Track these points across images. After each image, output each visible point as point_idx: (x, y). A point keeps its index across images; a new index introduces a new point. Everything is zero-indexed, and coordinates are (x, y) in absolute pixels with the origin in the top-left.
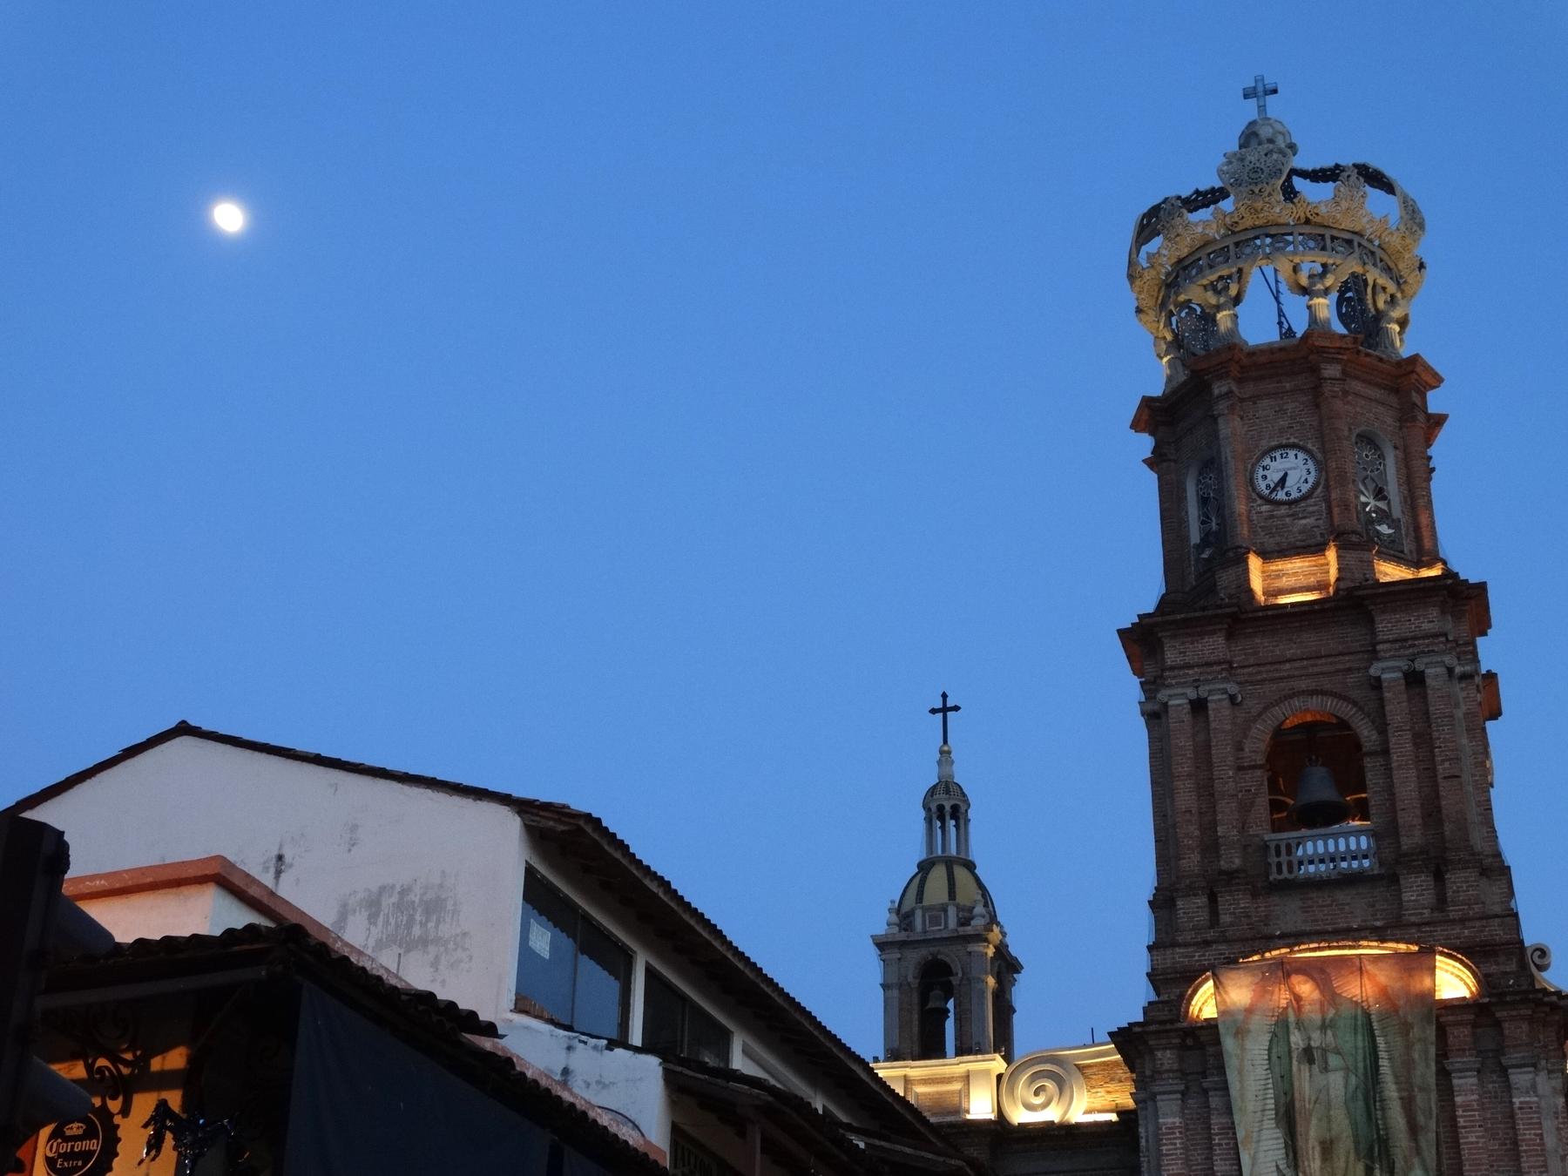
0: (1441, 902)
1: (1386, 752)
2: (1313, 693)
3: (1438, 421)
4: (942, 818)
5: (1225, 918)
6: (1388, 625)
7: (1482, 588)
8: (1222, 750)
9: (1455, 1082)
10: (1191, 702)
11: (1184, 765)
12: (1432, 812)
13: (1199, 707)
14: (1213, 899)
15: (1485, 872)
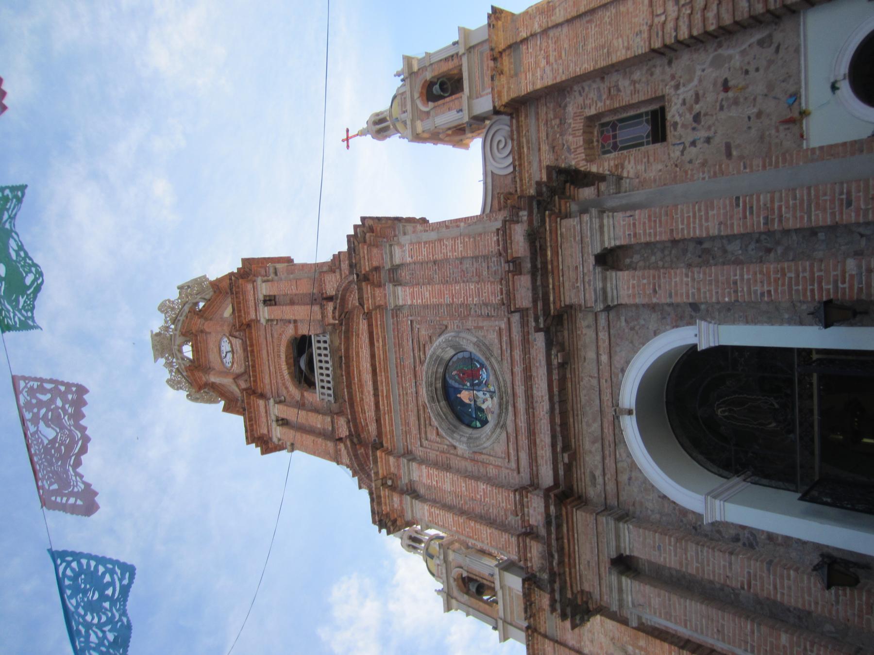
1: (295, 321)
2: (279, 356)
7: (244, 261)
9: (401, 303)
13: (283, 422)
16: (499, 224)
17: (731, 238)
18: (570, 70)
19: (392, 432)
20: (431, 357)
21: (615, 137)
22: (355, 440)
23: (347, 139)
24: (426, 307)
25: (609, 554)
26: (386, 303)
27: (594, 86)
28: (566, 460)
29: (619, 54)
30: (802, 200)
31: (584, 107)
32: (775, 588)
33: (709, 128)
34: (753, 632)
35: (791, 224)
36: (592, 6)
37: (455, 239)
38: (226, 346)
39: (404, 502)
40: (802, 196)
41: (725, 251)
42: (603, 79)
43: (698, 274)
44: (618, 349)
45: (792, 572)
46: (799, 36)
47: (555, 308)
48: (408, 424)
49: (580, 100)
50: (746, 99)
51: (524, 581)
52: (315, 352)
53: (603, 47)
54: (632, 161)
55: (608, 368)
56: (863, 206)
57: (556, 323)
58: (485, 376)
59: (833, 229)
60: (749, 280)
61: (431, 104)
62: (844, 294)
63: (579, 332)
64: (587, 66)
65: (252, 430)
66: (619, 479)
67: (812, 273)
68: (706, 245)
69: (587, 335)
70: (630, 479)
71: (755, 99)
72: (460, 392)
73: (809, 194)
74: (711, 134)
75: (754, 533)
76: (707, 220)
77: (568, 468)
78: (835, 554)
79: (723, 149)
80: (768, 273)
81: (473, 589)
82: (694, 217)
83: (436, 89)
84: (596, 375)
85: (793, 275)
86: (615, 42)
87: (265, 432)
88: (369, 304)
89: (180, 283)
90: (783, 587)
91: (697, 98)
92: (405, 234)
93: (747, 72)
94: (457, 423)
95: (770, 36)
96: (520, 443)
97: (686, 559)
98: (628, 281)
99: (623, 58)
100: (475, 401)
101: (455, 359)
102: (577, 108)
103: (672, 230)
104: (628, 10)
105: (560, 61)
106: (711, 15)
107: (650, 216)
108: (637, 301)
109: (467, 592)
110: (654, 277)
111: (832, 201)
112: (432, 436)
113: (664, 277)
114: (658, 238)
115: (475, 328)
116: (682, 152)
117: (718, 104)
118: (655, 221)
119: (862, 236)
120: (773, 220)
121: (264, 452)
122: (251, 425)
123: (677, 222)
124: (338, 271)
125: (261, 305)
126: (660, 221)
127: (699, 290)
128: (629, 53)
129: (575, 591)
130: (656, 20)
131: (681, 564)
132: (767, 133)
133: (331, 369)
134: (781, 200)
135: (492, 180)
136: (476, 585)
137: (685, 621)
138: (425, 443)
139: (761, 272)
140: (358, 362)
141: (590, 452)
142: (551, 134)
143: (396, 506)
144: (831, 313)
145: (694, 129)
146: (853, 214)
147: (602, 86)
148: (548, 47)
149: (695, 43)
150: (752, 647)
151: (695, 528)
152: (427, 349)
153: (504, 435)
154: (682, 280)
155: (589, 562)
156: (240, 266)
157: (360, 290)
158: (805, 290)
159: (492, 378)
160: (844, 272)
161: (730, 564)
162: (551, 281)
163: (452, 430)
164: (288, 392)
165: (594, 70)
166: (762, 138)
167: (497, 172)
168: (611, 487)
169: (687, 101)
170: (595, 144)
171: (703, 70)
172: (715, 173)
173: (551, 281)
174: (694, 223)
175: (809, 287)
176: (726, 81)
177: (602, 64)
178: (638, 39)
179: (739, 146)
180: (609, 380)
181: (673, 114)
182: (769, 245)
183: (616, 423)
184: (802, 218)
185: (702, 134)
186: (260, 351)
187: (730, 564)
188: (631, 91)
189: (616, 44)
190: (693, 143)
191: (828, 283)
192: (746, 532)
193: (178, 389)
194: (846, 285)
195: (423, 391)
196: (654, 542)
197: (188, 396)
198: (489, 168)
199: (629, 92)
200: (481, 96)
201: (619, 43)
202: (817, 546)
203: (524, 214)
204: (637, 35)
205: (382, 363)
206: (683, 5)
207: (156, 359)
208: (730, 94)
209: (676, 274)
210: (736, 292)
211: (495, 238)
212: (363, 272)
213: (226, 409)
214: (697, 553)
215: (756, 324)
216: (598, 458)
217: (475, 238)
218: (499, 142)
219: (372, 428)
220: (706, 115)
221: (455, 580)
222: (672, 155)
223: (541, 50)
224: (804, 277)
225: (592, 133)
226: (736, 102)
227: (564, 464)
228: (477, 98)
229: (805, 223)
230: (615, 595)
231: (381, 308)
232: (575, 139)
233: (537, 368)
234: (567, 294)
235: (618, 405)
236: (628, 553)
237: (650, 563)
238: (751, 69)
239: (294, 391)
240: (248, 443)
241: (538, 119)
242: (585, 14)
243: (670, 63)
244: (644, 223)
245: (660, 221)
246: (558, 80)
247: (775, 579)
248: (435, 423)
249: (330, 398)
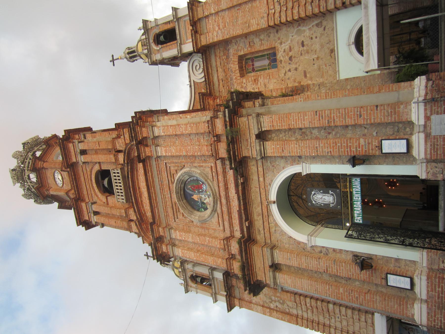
1: (99, 163)
2: (91, 180)
9: (160, 155)
10: (94, 215)
13: (96, 213)
16: (208, 118)
17: (313, 128)
18: (231, 33)
19: (159, 216)
20: (177, 180)
21: (253, 65)
22: (140, 221)
23: (113, 61)
24: (173, 157)
25: (268, 263)
26: (152, 155)
27: (242, 40)
28: (247, 225)
29: (254, 27)
30: (342, 114)
31: (238, 50)
32: (337, 270)
33: (296, 63)
34: (329, 289)
35: (338, 124)
36: (240, 2)
37: (186, 125)
38: (58, 177)
39: (169, 248)
40: (342, 112)
41: (312, 133)
42: (246, 37)
43: (302, 144)
44: (267, 175)
45: (343, 264)
46: (333, 23)
47: (238, 158)
48: (167, 212)
49: (236, 47)
50: (312, 51)
51: (223, 274)
52: (113, 178)
53: (246, 23)
54: (262, 78)
55: (263, 183)
56: (366, 118)
57: (240, 165)
58: (204, 188)
59: (355, 126)
60: (322, 146)
61: (160, 46)
62: (360, 153)
63: (249, 168)
64: (239, 32)
65: (80, 219)
66: (271, 231)
67: (347, 144)
68: (303, 131)
69: (253, 169)
70: (275, 231)
71: (316, 51)
72: (193, 196)
73: (345, 111)
74: (297, 66)
75: (327, 249)
76: (304, 120)
77: (248, 228)
78: (359, 254)
79: (303, 73)
80: (330, 144)
81: (199, 280)
82: (299, 119)
83: (162, 38)
84: (258, 187)
85: (340, 145)
86: (251, 20)
87: (87, 218)
88: (143, 156)
89: (23, 142)
90: (340, 270)
91: (290, 50)
92: (158, 121)
93: (312, 38)
94: (191, 209)
95: (321, 22)
96: (224, 218)
97: (301, 262)
98: (271, 146)
99: (256, 29)
100: (201, 200)
101: (189, 180)
102: (235, 52)
103: (289, 124)
104: (257, 5)
105: (226, 29)
106: (295, 11)
107: (279, 118)
108: (275, 155)
109: (196, 282)
110: (282, 145)
111: (354, 115)
112: (180, 217)
113: (287, 145)
114: (283, 128)
115: (199, 166)
116: (285, 75)
117: (300, 52)
118: (282, 120)
119: (365, 128)
120: (331, 121)
121: (86, 229)
122: (79, 216)
123: (291, 121)
124: (122, 137)
125: (79, 155)
126: (284, 120)
127: (302, 150)
128: (258, 27)
129: (254, 281)
130: (270, 11)
131: (299, 264)
132: (322, 67)
133: (123, 186)
134: (334, 113)
135: (194, 85)
136: (200, 278)
137: (302, 287)
138: (177, 220)
139: (327, 143)
140: (138, 183)
141: (257, 220)
142: (222, 63)
143: (164, 251)
144: (355, 161)
145: (289, 64)
146: (362, 121)
147: (246, 41)
148: (218, 20)
149: (289, 23)
150: (329, 294)
151: (304, 249)
152: (175, 176)
153: (216, 215)
154: (294, 146)
155: (260, 268)
156: (64, 134)
157: (138, 149)
158: (345, 151)
159: (208, 188)
160: (359, 144)
161: (319, 263)
162: (236, 146)
163: (191, 213)
164: (98, 198)
165: (242, 34)
166: (319, 69)
167: (196, 80)
168: (267, 235)
169: (286, 50)
170: (244, 68)
171: (293, 36)
172: (306, 98)
173: (236, 146)
174: (299, 122)
175: (346, 150)
176: (303, 42)
177: (246, 31)
178: (262, 21)
179: (310, 72)
180: (264, 189)
181: (280, 55)
182: (329, 131)
183: (268, 206)
184: (342, 121)
185: (293, 66)
186: (79, 178)
187: (319, 263)
188: (260, 45)
189: (252, 22)
190: (290, 70)
191: (353, 148)
192: (325, 249)
193: (29, 199)
194: (360, 149)
195: (174, 196)
196: (288, 256)
197: (35, 201)
198: (193, 78)
199: (259, 45)
200: (186, 43)
201: (253, 22)
202: (352, 252)
203: (220, 114)
204: (262, 18)
205: (152, 183)
206: (282, 6)
207: (14, 184)
208: (305, 48)
209: (291, 143)
210: (317, 151)
211: (207, 125)
212: (139, 140)
213: (60, 207)
214: (306, 260)
215: (325, 164)
216: (261, 222)
217: (196, 124)
218: (196, 66)
219: (149, 214)
220: (294, 57)
221: (190, 278)
222: (280, 75)
223: (215, 22)
224: (344, 146)
225: (242, 63)
226: (308, 52)
227: (246, 227)
228: (184, 44)
229: (344, 124)
230: (272, 280)
231: (149, 158)
232: (234, 66)
233: (230, 184)
234: (243, 152)
235: (268, 199)
236: (276, 262)
237: (285, 265)
238: (314, 37)
239: (102, 198)
240: (78, 225)
241: (216, 56)
242: (236, 6)
243: (277, 32)
244: (277, 121)
245: (284, 120)
246: (225, 38)
247: (337, 267)
248: (182, 211)
249: (123, 201)
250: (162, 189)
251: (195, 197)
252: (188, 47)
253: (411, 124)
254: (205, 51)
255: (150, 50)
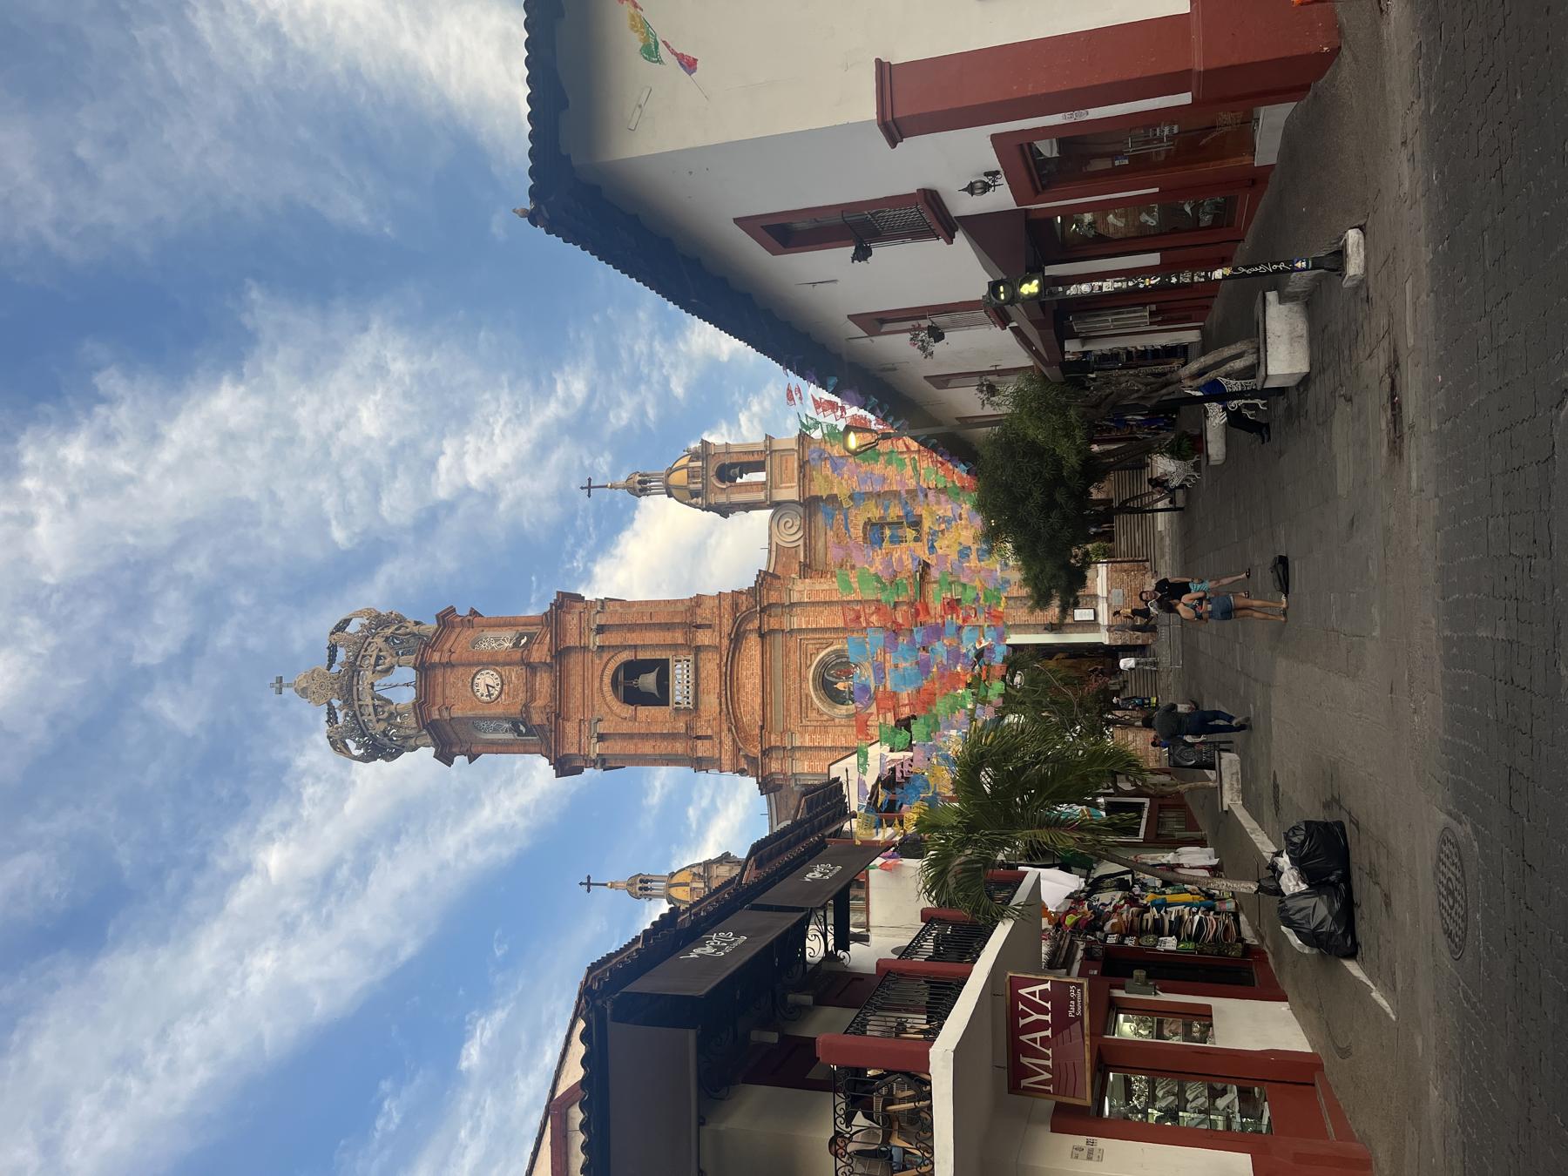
0: (709, 626)
1: (635, 647)
3: (474, 613)
4: (646, 889)
5: (709, 732)
6: (572, 640)
8: (625, 728)
11: (630, 748)
12: (668, 627)
13: (601, 738)
14: (699, 738)
15: (698, 605)
23: (589, 487)
87: (573, 750)
88: (765, 628)
112: (814, 715)
198: (775, 539)
250: (785, 676)
251: (840, 686)
252: (789, 493)
253: (1096, 596)
254: (810, 505)
255: (705, 486)
